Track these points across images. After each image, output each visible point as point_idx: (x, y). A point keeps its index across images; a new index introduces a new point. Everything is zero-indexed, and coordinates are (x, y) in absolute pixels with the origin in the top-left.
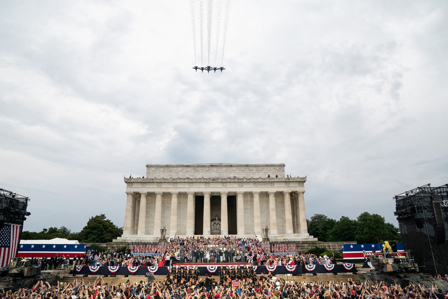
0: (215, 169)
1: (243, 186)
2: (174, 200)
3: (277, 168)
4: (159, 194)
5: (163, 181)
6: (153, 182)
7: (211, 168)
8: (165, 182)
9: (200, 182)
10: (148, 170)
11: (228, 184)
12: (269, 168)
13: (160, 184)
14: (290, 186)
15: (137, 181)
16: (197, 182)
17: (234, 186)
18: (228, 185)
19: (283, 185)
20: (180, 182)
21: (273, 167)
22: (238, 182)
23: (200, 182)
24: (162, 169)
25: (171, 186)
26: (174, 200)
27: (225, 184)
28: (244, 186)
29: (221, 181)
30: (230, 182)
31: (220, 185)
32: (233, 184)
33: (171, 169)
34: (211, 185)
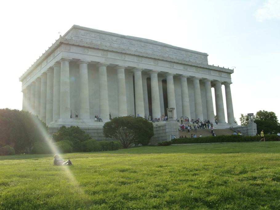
0: (151, 46)
1: (187, 69)
5: (111, 49)
6: (98, 49)
8: (112, 51)
11: (175, 65)
12: (197, 55)
13: (105, 53)
15: (77, 44)
19: (217, 74)
20: (130, 55)
21: (199, 55)
24: (93, 35)
27: (172, 64)
28: (188, 70)
29: (170, 60)
33: (104, 36)
34: (160, 63)
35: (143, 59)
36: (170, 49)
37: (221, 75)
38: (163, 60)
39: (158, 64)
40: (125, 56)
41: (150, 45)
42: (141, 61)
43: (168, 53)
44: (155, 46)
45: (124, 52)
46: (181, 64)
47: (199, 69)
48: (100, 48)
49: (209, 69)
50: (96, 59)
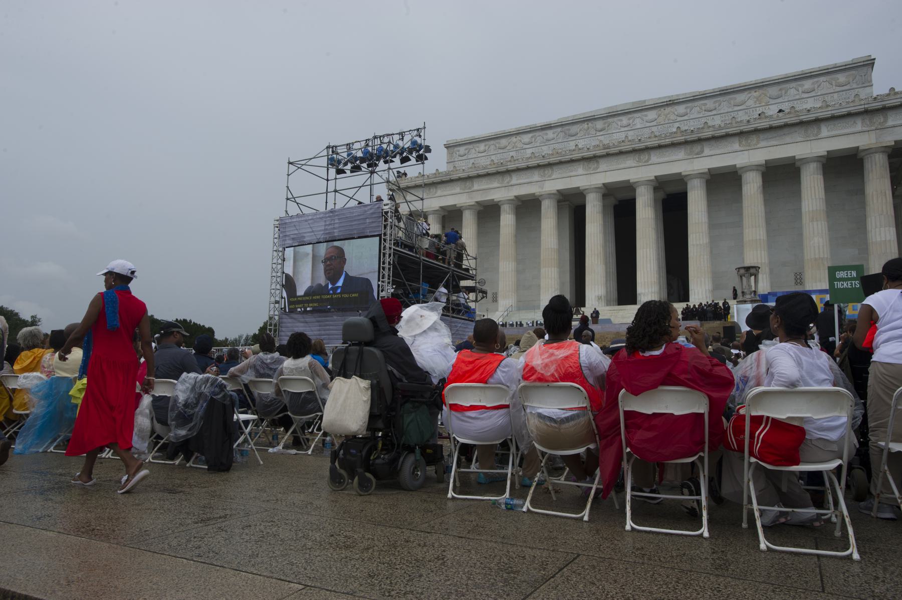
1: (702, 152)
2: (507, 220)
3: (842, 78)
4: (470, 207)
6: (451, 181)
7: (610, 120)
8: (479, 176)
9: (572, 161)
10: (450, 154)
12: (808, 84)
13: (468, 184)
14: (890, 122)
16: (561, 163)
17: (674, 158)
18: (655, 157)
19: (858, 125)
20: (518, 170)
21: (822, 79)
22: (686, 143)
23: (572, 161)
24: (482, 147)
25: (496, 185)
26: (507, 220)
27: (644, 157)
28: (707, 151)
29: (628, 147)
30: (660, 147)
31: (630, 161)
32: (669, 151)
33: (504, 142)
34: (603, 165)
35: (555, 168)
36: (690, 105)
37: (886, 121)
38: (608, 155)
39: (597, 168)
40: (511, 176)
41: (620, 118)
42: (550, 176)
43: (679, 119)
44: (639, 115)
45: (502, 169)
46: (673, 145)
47: (754, 139)
48: (454, 177)
49: (801, 123)
50: (449, 201)
